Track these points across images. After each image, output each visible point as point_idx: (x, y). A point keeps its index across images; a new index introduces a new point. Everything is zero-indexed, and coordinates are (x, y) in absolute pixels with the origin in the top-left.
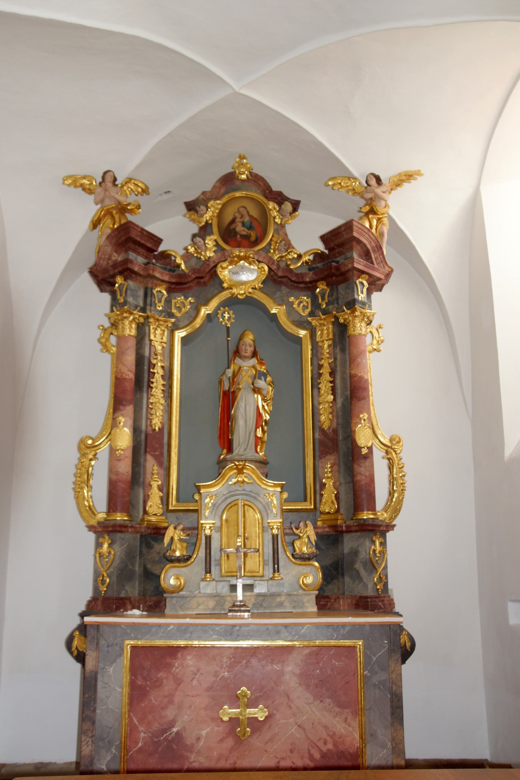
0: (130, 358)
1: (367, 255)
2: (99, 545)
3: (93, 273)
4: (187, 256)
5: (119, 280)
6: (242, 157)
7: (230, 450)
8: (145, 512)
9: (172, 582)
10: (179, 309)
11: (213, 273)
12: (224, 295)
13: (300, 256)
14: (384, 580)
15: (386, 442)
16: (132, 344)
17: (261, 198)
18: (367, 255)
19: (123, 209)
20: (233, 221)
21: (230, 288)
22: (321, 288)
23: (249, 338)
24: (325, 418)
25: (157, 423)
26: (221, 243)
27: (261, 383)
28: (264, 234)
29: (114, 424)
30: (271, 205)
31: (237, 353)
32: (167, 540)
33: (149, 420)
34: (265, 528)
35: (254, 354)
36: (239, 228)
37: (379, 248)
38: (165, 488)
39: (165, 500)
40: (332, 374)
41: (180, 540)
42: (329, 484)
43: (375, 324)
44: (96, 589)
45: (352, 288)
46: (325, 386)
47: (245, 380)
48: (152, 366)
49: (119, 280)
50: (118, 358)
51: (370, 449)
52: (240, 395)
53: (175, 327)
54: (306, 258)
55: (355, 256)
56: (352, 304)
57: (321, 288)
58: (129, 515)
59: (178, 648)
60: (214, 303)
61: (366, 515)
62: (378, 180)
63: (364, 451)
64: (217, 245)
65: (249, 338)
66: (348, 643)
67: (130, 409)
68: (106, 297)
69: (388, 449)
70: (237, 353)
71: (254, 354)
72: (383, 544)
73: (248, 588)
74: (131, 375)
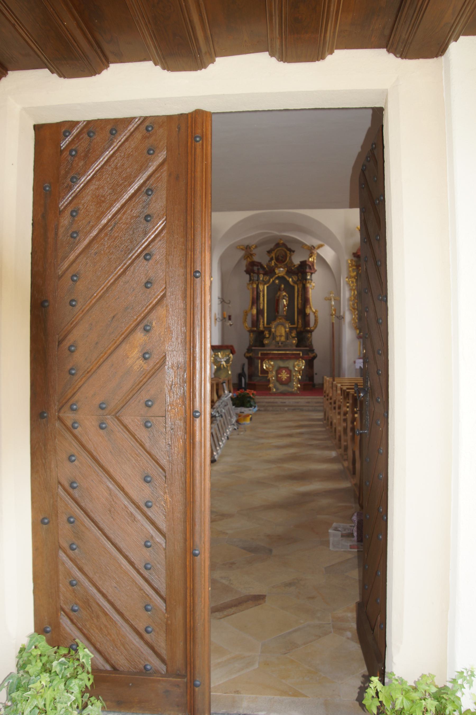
0: (255, 293)
1: (310, 268)
2: (250, 335)
3: (245, 271)
4: (267, 266)
5: (252, 274)
6: (281, 239)
7: (278, 313)
8: (259, 327)
9: (266, 342)
10: (265, 279)
11: (274, 270)
12: (277, 276)
13: (295, 265)
14: (311, 342)
15: (314, 311)
16: (255, 290)
17: (285, 250)
18: (310, 268)
19: (251, 255)
20: (278, 256)
21: (278, 274)
22: (300, 274)
23: (283, 286)
24: (300, 306)
25: (261, 307)
26: (276, 262)
27: (285, 298)
28: (286, 259)
29: (252, 308)
30: (288, 252)
31: (280, 289)
32: (265, 334)
33: (260, 306)
34: (285, 331)
35: (284, 290)
36: (280, 258)
37: (313, 265)
38: (263, 322)
39: (264, 325)
40: (302, 296)
41: (268, 334)
42: (300, 321)
43: (313, 281)
44: (250, 344)
45: (306, 276)
46: (300, 299)
47: (281, 297)
48: (260, 294)
49: (252, 274)
50: (253, 292)
51: (309, 314)
52: (280, 300)
53: (265, 284)
54: (296, 266)
55: (308, 267)
56: (306, 279)
57: (300, 274)
58: (257, 328)
59: (268, 353)
60: (273, 279)
61: (309, 329)
62: (314, 248)
63: (308, 314)
64: (274, 263)
65: (283, 286)
66: (298, 352)
67: (255, 305)
68: (248, 276)
69: (314, 313)
70: (280, 289)
71: (284, 290)
72: (311, 335)
73: (282, 343)
74: (255, 297)
